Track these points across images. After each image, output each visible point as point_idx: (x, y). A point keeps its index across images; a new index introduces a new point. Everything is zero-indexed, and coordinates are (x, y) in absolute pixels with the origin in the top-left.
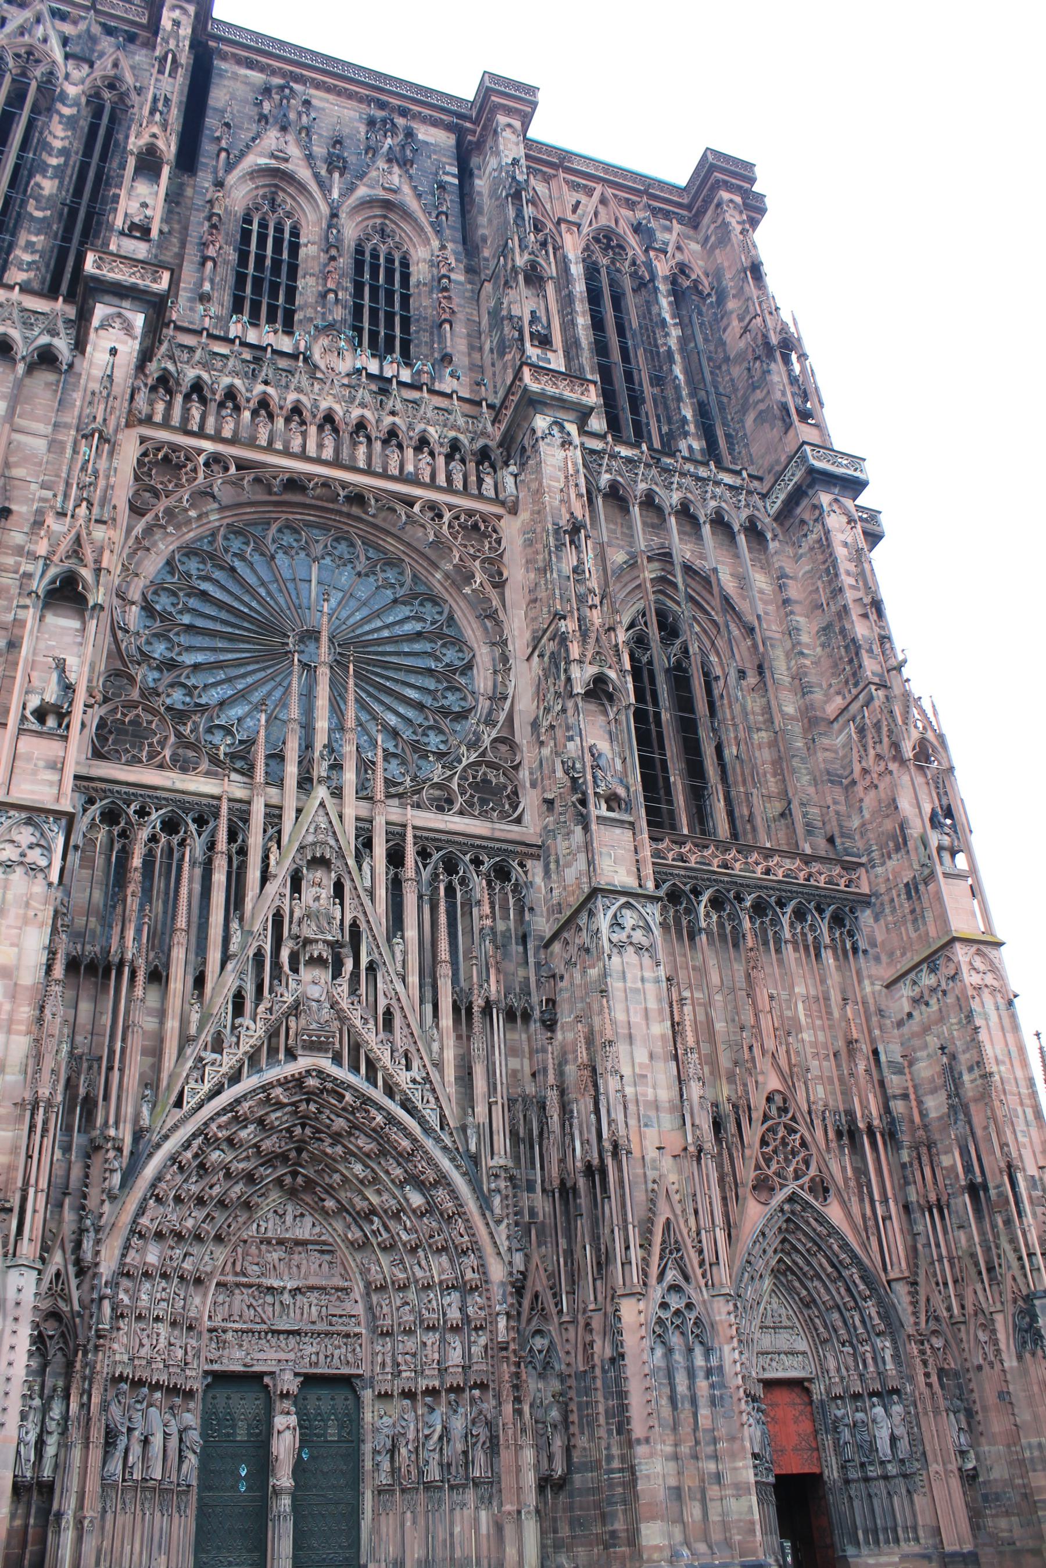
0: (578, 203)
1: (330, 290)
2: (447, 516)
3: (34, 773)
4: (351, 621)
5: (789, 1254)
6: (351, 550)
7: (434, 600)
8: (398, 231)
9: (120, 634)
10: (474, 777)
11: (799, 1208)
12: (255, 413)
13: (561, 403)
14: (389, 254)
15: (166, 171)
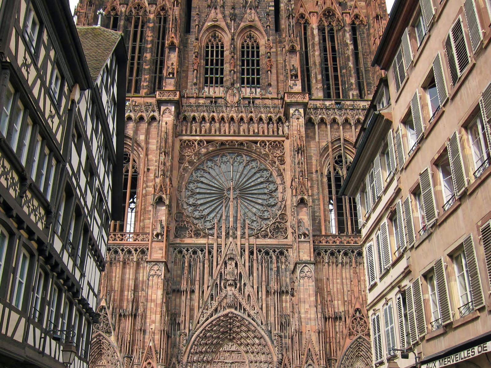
0: (317, 2)
1: (232, 70)
2: (268, 144)
3: (157, 252)
4: (243, 182)
5: (361, 352)
6: (242, 158)
7: (266, 170)
8: (255, 35)
9: (179, 201)
10: (274, 227)
11: (362, 340)
12: (211, 123)
13: (297, 104)
14: (253, 45)
15: (177, 49)
